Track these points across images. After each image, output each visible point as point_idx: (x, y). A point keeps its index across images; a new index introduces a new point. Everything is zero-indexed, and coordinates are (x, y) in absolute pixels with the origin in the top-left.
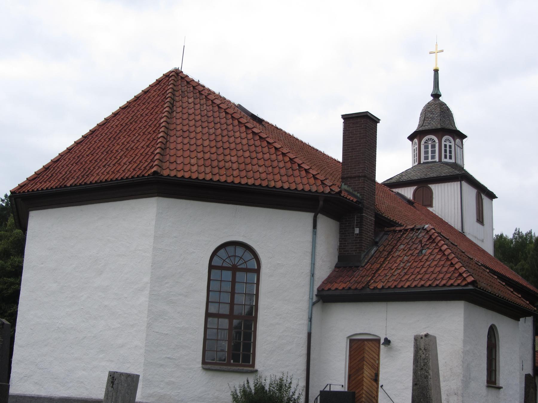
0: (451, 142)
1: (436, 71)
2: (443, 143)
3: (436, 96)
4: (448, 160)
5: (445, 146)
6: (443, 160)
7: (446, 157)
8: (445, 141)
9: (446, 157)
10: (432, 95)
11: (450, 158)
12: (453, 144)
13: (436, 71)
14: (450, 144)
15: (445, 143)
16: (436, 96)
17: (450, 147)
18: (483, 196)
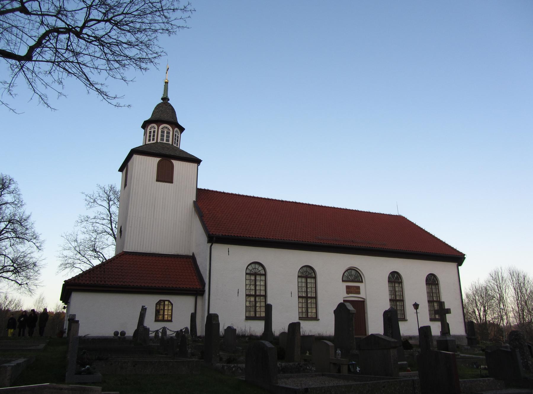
0: (155, 129)
1: (167, 83)
2: (148, 131)
3: (165, 99)
4: (152, 142)
5: (150, 132)
6: (148, 142)
7: (150, 140)
8: (150, 129)
9: (150, 140)
10: (162, 99)
11: (153, 140)
12: (156, 130)
13: (167, 83)
14: (154, 130)
15: (150, 130)
16: (165, 99)
17: (154, 132)
18: (174, 162)
